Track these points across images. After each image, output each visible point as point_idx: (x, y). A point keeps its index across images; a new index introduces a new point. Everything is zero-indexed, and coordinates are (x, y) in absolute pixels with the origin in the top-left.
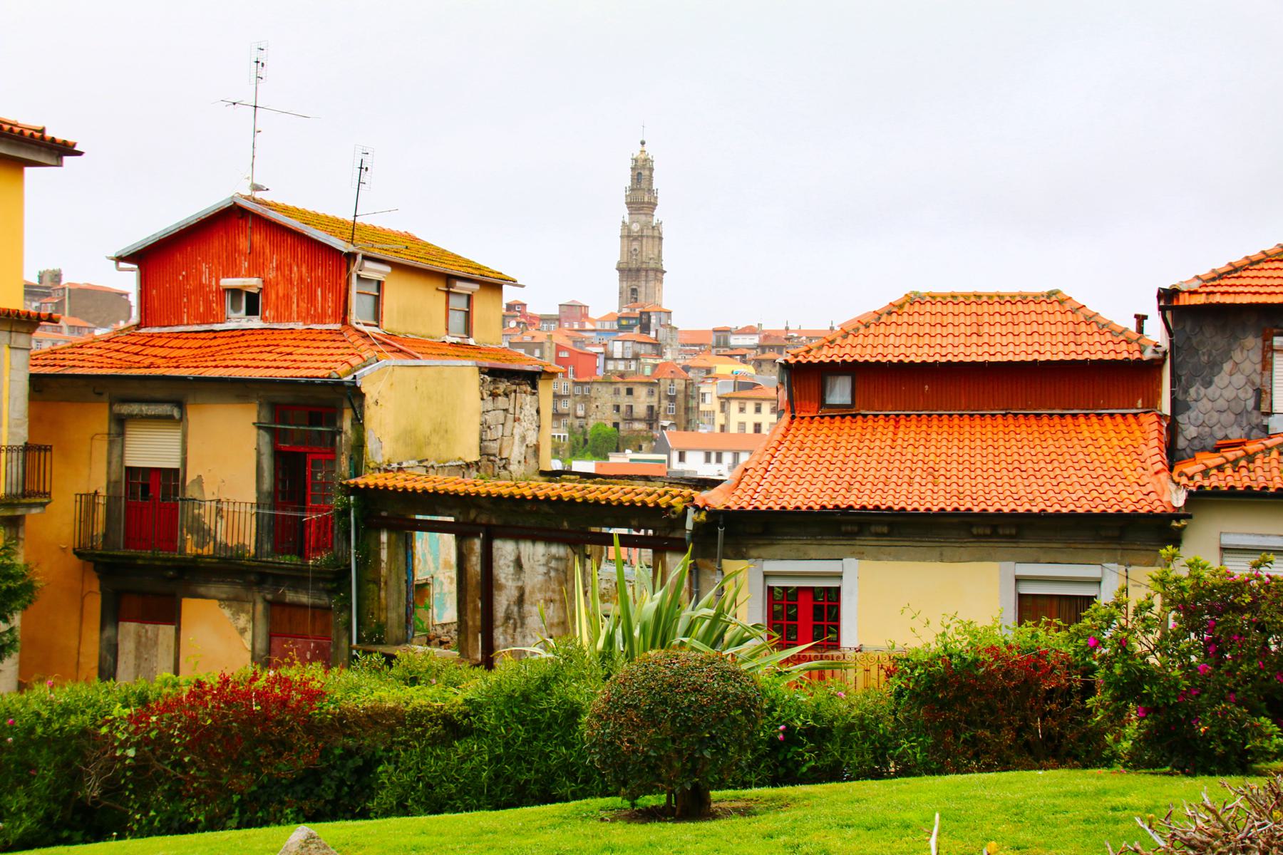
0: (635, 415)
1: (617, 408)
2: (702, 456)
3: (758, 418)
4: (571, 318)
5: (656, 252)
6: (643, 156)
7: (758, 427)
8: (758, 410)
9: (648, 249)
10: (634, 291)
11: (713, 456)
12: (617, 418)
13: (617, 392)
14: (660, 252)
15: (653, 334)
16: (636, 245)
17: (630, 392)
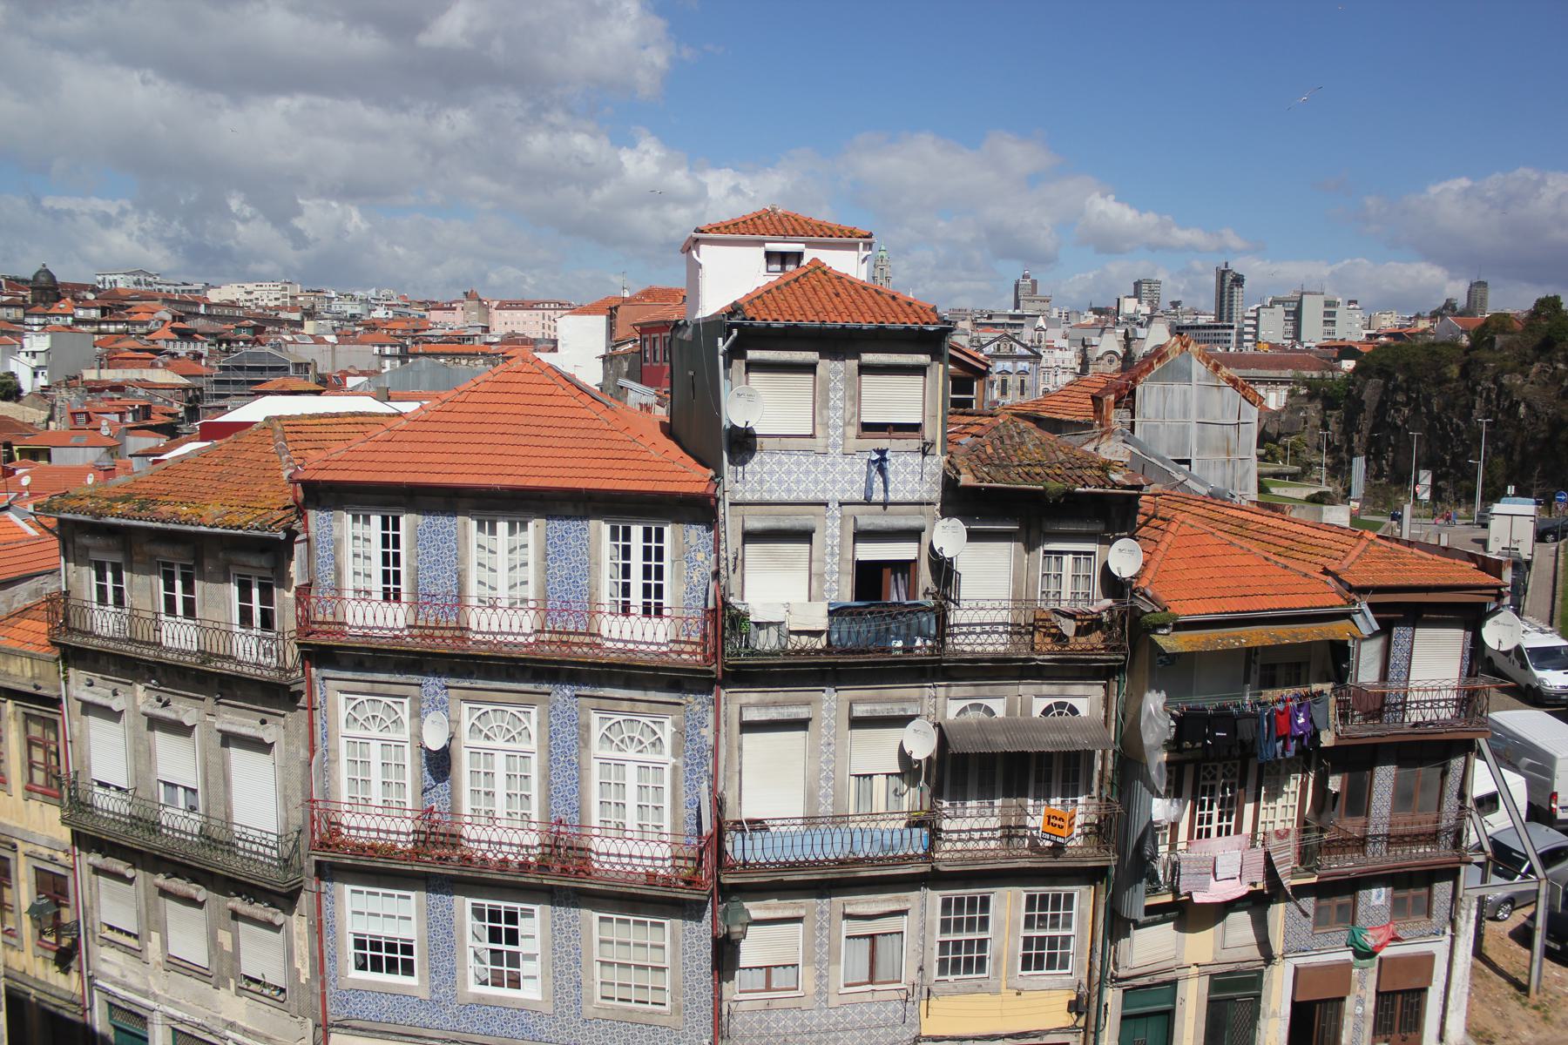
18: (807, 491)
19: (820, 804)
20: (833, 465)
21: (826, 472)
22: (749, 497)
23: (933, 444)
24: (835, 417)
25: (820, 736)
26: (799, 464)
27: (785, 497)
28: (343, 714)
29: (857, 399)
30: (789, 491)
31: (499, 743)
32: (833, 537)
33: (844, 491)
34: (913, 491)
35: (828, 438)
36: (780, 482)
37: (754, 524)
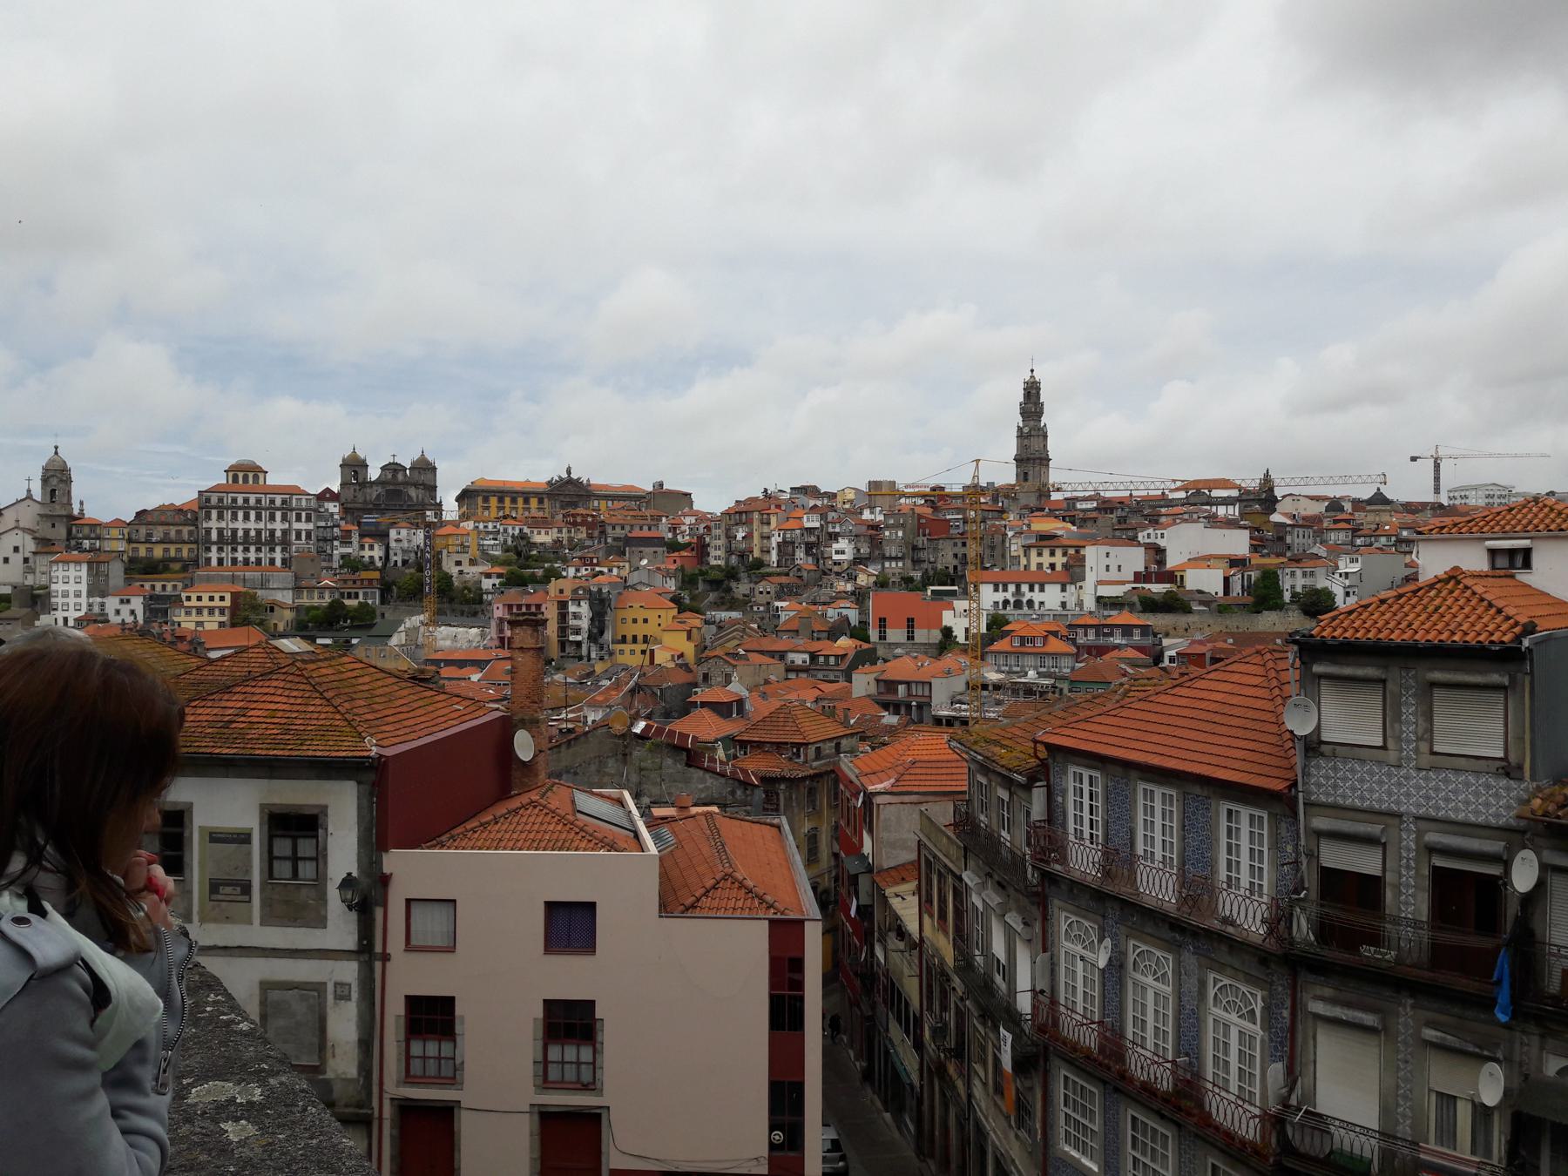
1: (956, 556)
2: (991, 587)
3: (1052, 560)
7: (1052, 566)
8: (1052, 554)
9: (1035, 444)
12: (955, 562)
13: (955, 545)
14: (1045, 446)
16: (1026, 442)
17: (964, 544)
18: (1380, 801)
19: (1397, 1123)
20: (1406, 778)
21: (1399, 784)
22: (1323, 799)
23: (1520, 767)
24: (1409, 731)
25: (1398, 1051)
26: (1372, 774)
27: (1358, 803)
28: (1064, 927)
29: (1429, 717)
30: (1362, 798)
31: (1150, 980)
32: (1409, 850)
33: (1419, 806)
34: (1497, 816)
35: (1401, 750)
36: (1354, 789)
37: (1321, 823)
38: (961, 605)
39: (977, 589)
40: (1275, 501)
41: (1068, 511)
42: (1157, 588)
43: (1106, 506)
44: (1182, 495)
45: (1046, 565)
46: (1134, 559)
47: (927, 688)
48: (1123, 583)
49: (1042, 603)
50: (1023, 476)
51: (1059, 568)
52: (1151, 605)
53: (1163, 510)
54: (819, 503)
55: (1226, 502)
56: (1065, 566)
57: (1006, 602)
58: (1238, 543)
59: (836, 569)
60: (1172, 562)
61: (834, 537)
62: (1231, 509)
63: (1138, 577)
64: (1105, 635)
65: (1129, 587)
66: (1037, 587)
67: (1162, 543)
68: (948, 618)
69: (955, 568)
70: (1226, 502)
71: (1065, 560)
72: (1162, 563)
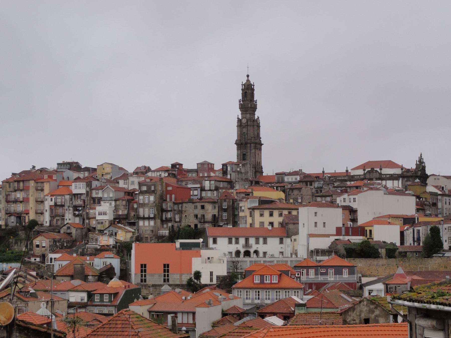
0: (206, 220)
1: (196, 216)
2: (226, 240)
3: (271, 219)
4: (203, 171)
5: (256, 134)
6: (248, 83)
7: (271, 224)
8: (271, 215)
10: (244, 155)
11: (234, 240)
12: (196, 221)
13: (196, 207)
14: (258, 134)
15: (229, 177)
16: (245, 130)
17: (203, 207)
38: (205, 253)
39: (215, 242)
40: (427, 177)
41: (278, 181)
42: (357, 239)
43: (308, 179)
44: (360, 172)
45: (266, 225)
46: (334, 218)
47: (191, 316)
48: (328, 236)
49: (265, 253)
50: (243, 157)
51: (276, 225)
52: (353, 252)
53: (348, 183)
54: (81, 175)
55: (393, 177)
56: (282, 224)
57: (238, 253)
58: (407, 206)
59: (99, 227)
60: (361, 221)
61: (98, 201)
62: (396, 182)
63: (339, 231)
64: (322, 274)
65: (333, 239)
66: (261, 240)
67: (354, 206)
68: (197, 264)
69: (196, 226)
70: (393, 177)
71: (281, 219)
72: (354, 220)
